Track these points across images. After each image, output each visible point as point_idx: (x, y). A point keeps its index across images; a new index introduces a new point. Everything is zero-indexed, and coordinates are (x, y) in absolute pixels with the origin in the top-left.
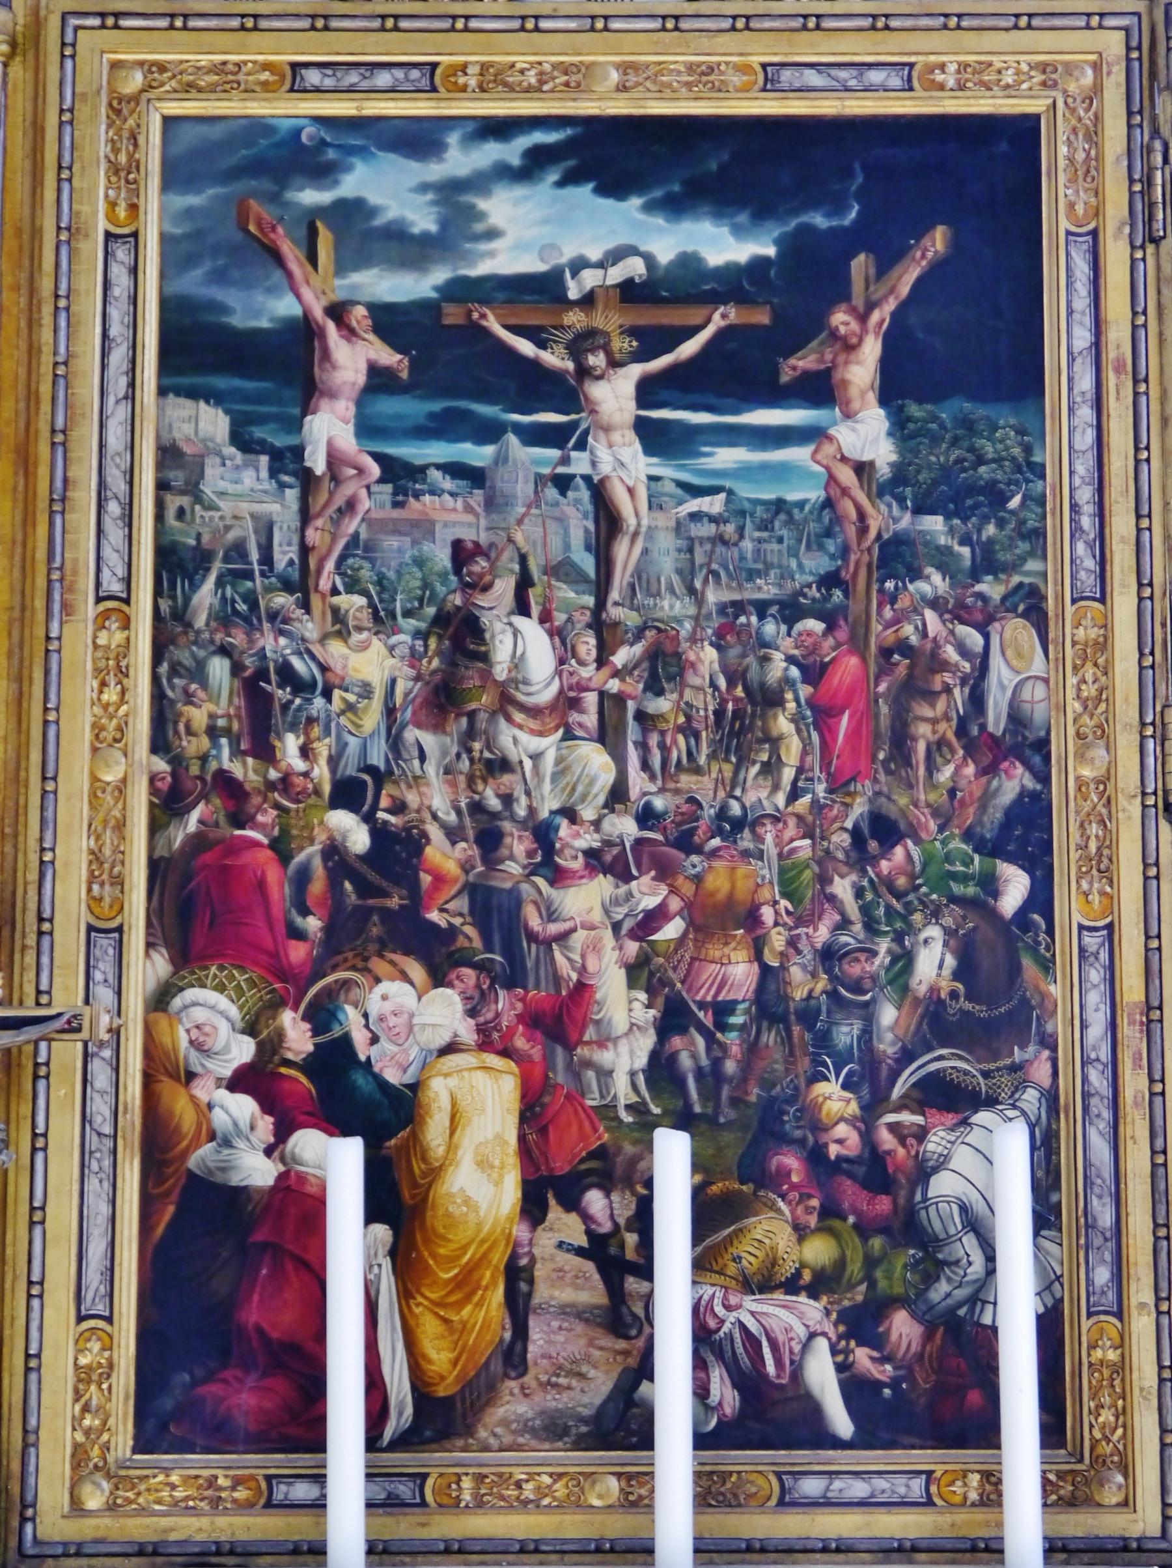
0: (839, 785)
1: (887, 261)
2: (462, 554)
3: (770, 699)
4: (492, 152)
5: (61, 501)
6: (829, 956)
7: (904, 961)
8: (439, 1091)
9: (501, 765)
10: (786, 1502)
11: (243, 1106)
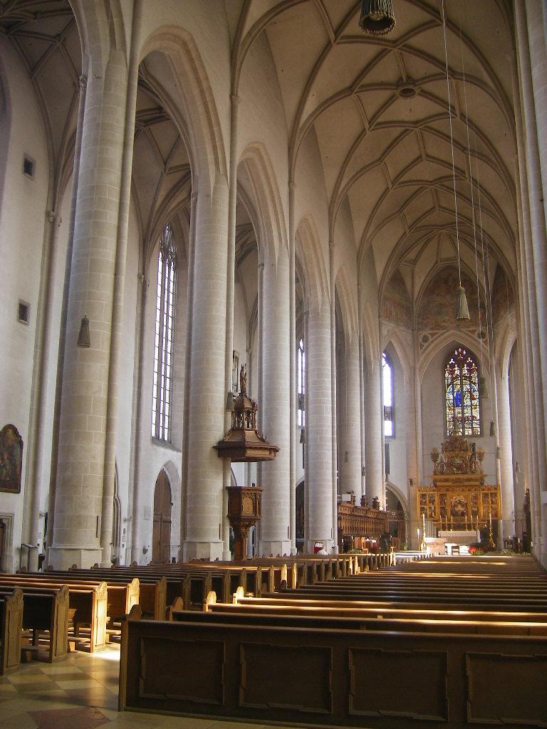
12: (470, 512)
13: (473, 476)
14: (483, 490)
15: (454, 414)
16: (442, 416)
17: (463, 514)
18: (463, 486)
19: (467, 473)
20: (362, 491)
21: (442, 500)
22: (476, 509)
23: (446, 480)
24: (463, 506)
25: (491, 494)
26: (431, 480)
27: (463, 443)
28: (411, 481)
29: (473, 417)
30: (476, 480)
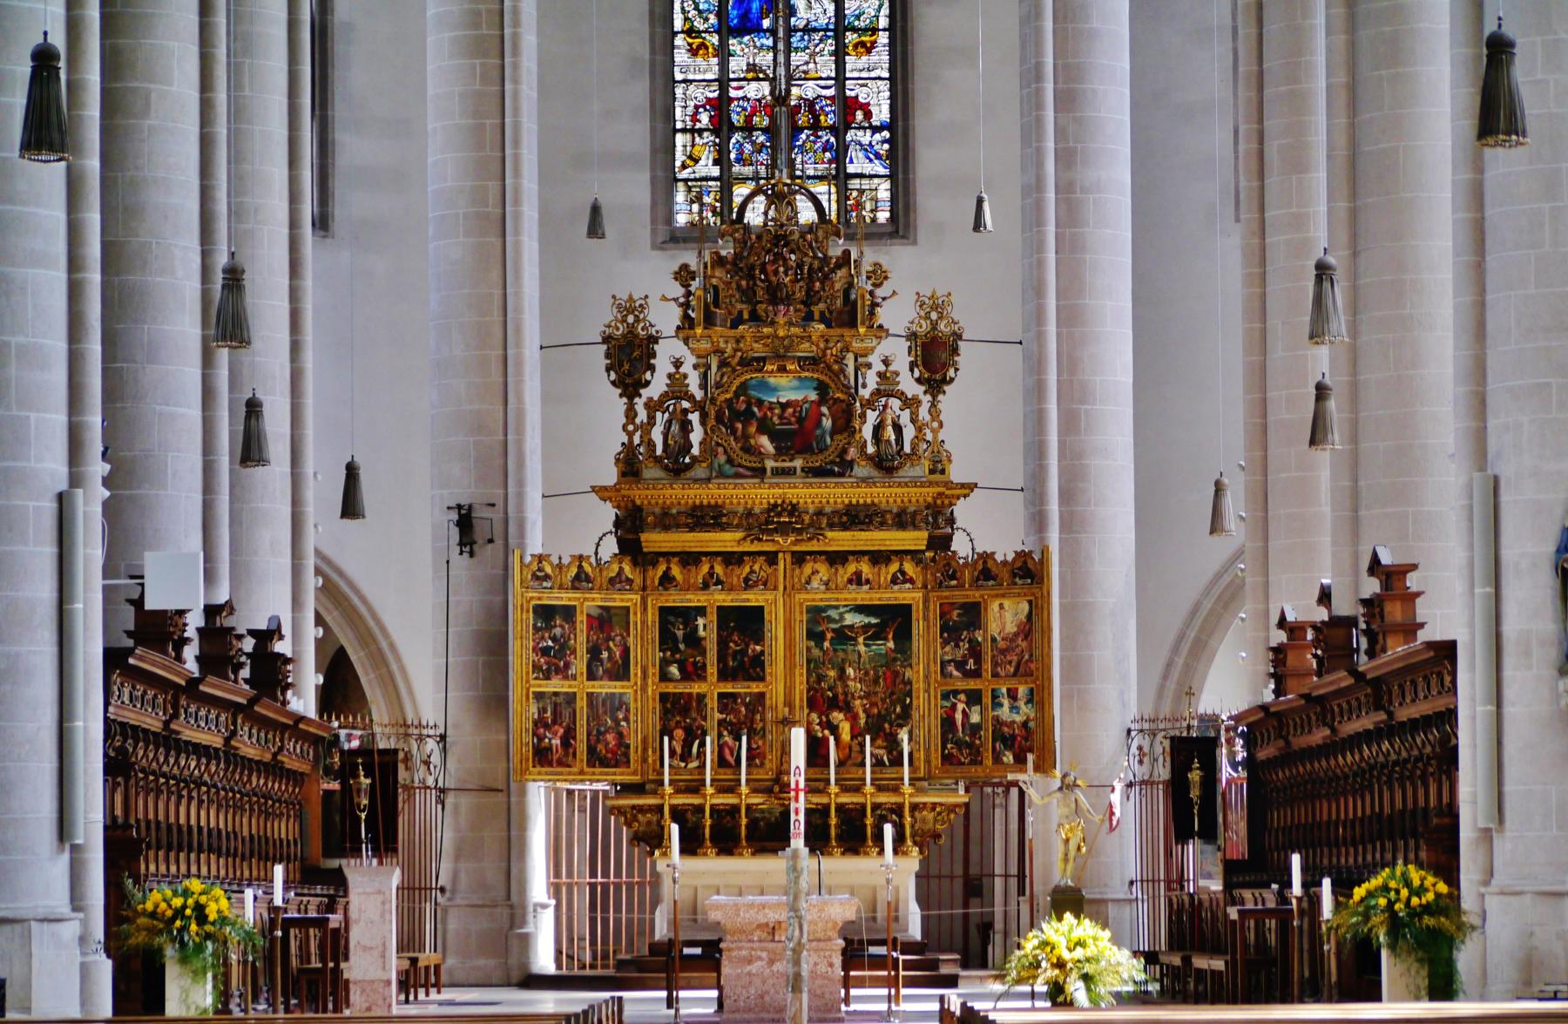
0: (888, 688)
1: (893, 622)
2: (843, 660)
3: (879, 677)
4: (846, 609)
5: (795, 654)
6: (886, 709)
7: (895, 709)
8: (841, 725)
9: (847, 686)
10: (881, 773)
11: (818, 728)
13: (884, 494)
16: (640, 91)
19: (843, 467)
20: (210, 576)
23: (706, 517)
26: (607, 514)
27: (825, 269)
28: (465, 521)
29: (849, 107)
30: (903, 520)
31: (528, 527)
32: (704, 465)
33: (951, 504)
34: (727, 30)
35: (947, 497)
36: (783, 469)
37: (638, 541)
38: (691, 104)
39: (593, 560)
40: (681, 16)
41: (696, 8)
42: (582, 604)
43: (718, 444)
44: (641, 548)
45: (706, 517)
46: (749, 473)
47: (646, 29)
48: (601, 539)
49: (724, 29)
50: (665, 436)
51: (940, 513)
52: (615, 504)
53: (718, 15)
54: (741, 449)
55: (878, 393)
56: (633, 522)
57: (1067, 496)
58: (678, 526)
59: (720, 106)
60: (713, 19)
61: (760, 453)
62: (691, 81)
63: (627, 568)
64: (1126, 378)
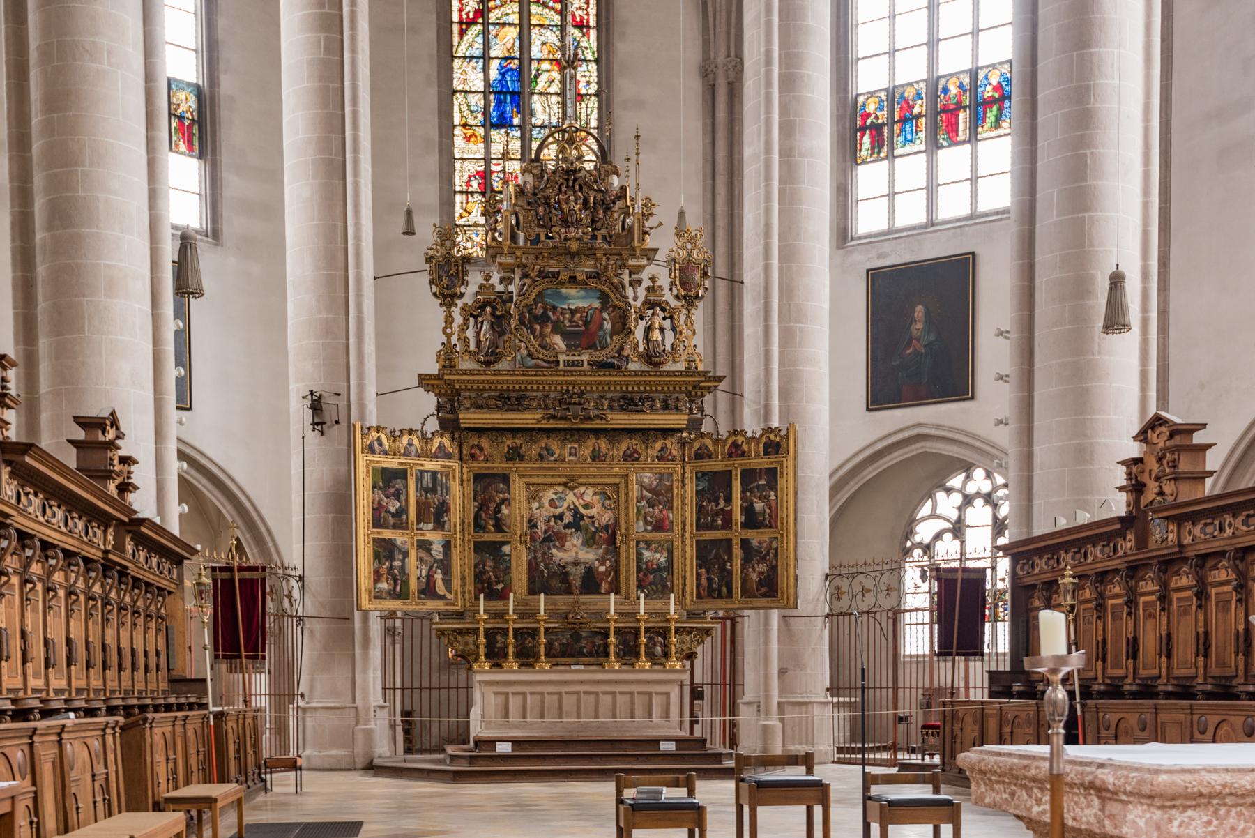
12: (629, 573)
14: (699, 456)
15: (487, 160)
17: (591, 582)
18: (597, 432)
21: (482, 506)
22: (661, 558)
23: (511, 400)
24: (590, 542)
25: (748, 476)
26: (429, 401)
31: (367, 412)
32: (509, 358)
33: (703, 396)
34: (489, 125)
35: (701, 388)
36: (573, 361)
37: (457, 420)
38: (466, 174)
39: (419, 433)
40: (459, 115)
41: (469, 109)
42: (412, 468)
43: (521, 341)
44: (459, 424)
45: (511, 400)
46: (546, 365)
47: (436, 120)
48: (426, 420)
49: (488, 124)
50: (478, 334)
51: (693, 401)
52: (437, 391)
53: (484, 114)
54: (539, 345)
55: (650, 304)
56: (452, 406)
57: (785, 394)
58: (488, 407)
59: (485, 175)
60: (480, 117)
61: (554, 349)
62: (466, 159)
63: (446, 442)
64: (826, 306)
